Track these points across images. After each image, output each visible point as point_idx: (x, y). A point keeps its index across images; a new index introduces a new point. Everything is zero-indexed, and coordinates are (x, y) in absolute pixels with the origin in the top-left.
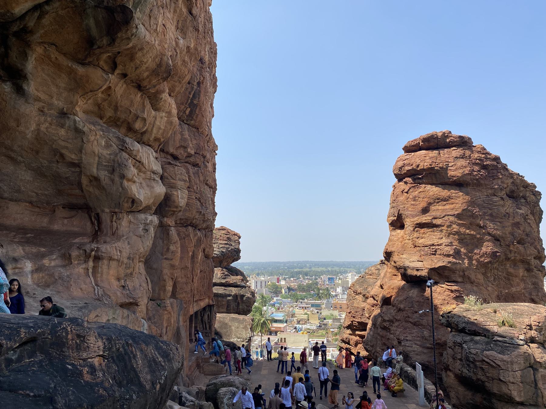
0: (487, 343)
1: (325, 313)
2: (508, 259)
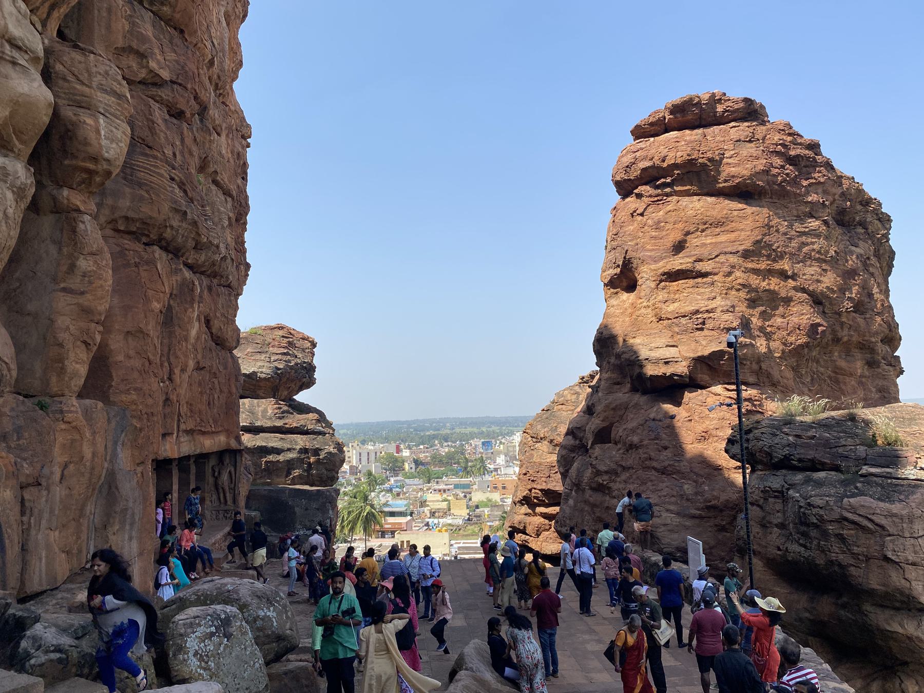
2: (837, 340)
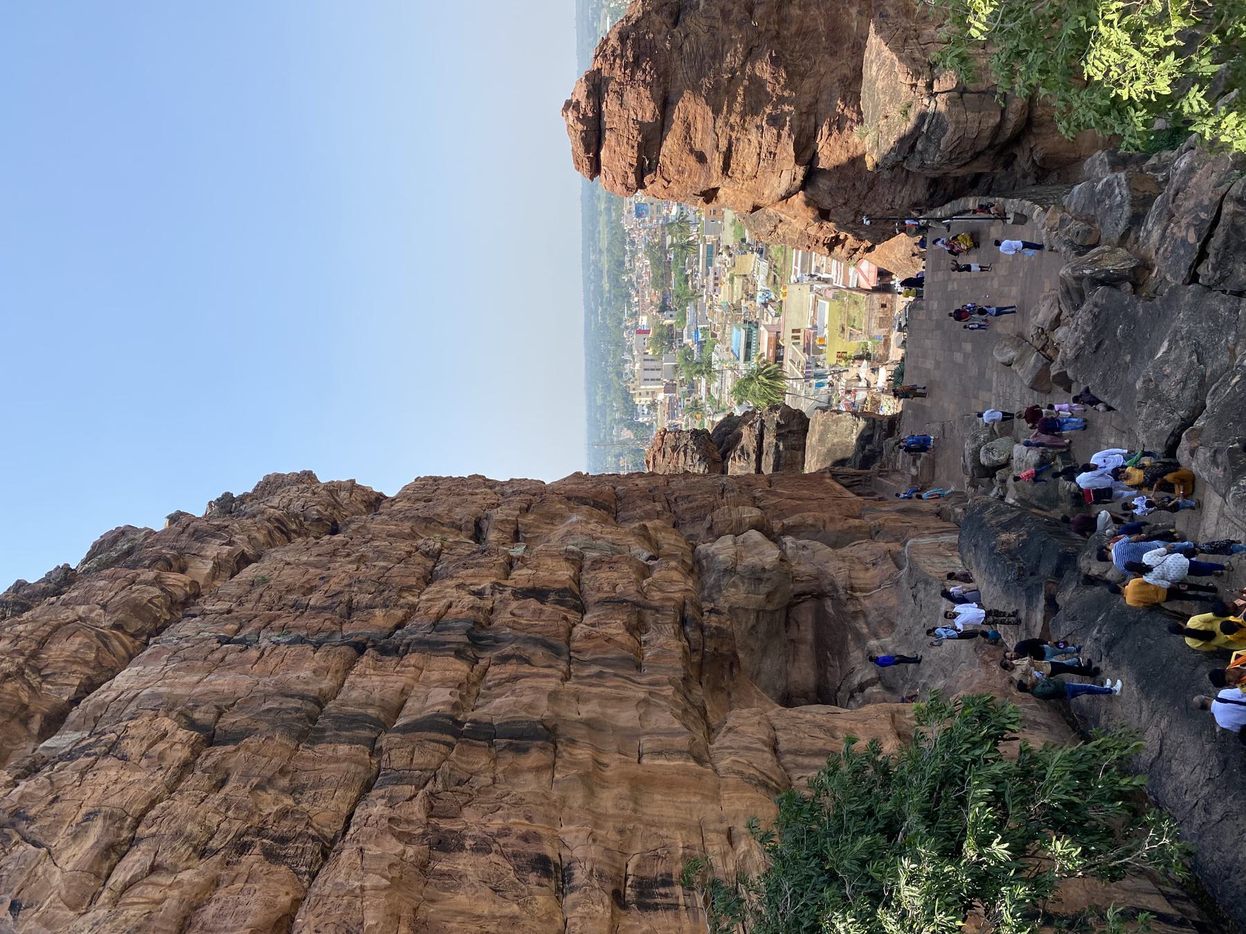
0: (928, 139)
1: (728, 238)
